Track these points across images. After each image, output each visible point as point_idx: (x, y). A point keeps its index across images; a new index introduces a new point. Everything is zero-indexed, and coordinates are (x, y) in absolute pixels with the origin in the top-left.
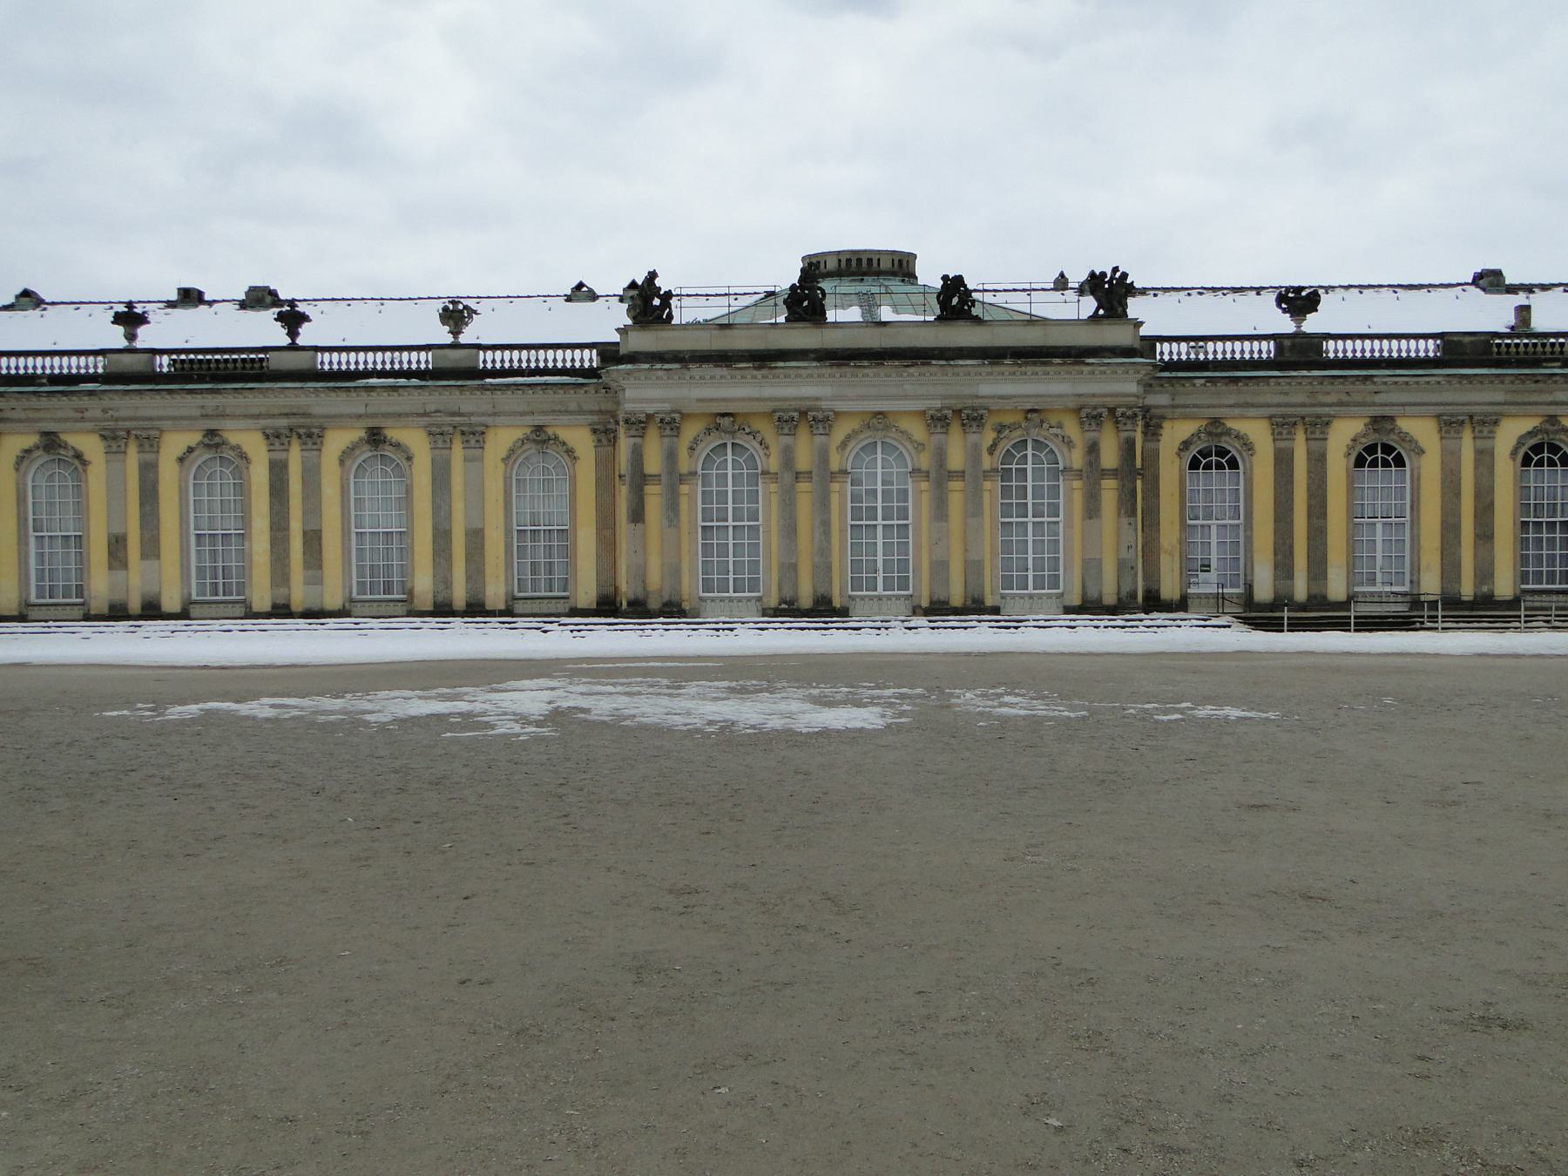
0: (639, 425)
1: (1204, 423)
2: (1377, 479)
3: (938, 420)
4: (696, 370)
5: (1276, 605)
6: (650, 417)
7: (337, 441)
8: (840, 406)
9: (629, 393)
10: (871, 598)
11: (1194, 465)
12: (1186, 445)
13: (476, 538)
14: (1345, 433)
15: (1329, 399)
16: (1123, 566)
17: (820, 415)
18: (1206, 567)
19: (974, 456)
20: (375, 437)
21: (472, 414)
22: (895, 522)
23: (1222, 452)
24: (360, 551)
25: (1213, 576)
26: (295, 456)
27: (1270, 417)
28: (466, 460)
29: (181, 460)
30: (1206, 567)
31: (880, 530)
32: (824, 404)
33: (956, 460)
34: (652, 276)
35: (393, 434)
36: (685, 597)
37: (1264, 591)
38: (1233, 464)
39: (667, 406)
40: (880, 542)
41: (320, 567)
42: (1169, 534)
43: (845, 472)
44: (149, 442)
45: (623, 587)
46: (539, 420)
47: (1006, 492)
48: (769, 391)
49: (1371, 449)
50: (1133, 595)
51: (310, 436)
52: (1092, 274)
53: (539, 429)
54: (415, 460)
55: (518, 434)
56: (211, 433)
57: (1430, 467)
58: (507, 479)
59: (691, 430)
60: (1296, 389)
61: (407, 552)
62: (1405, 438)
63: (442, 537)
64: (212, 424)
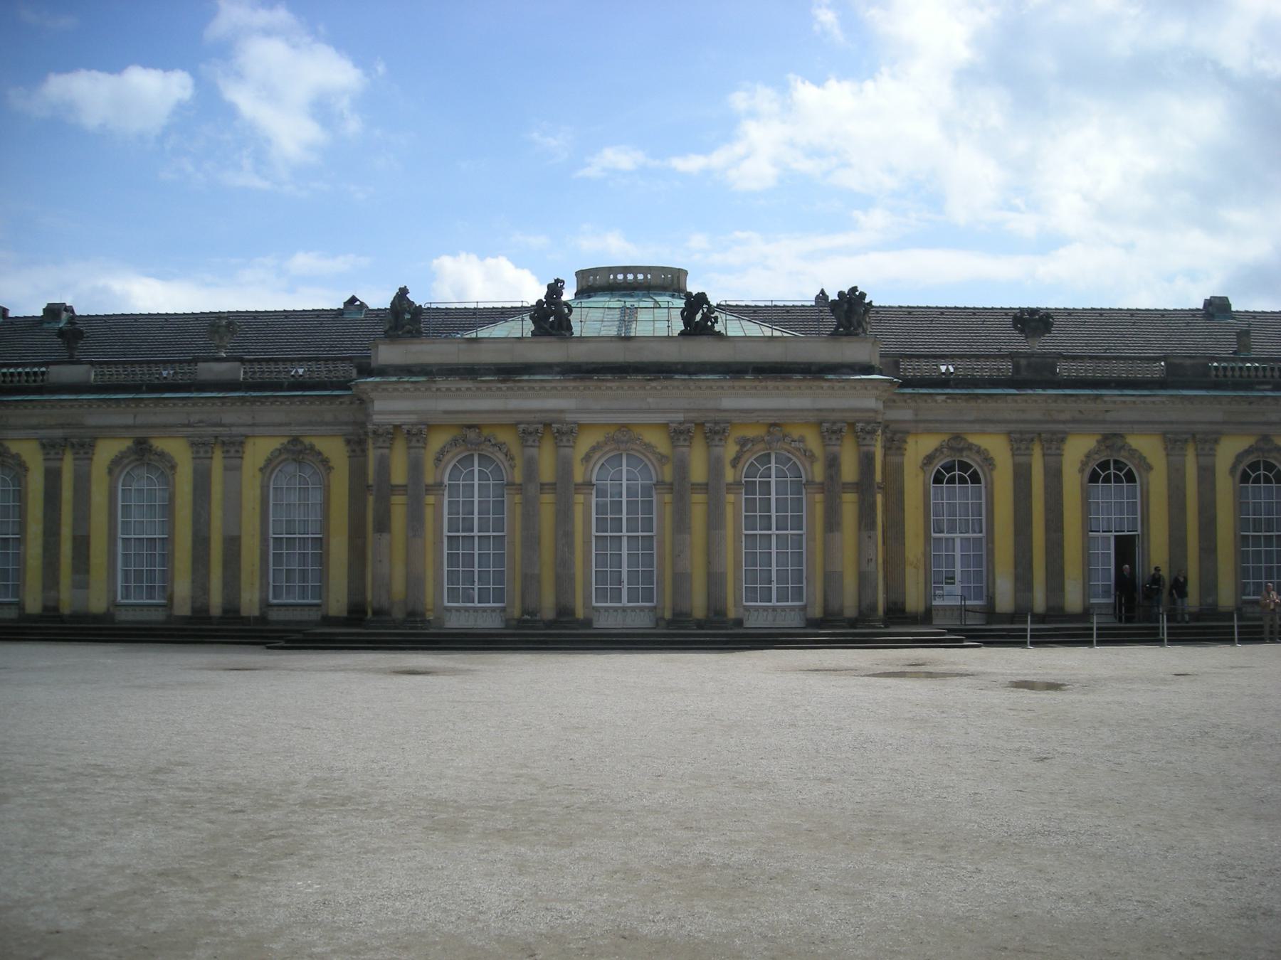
1: (946, 438)
3: (678, 434)
4: (442, 383)
5: (1018, 615)
6: (397, 427)
7: (107, 450)
8: (584, 418)
9: (378, 405)
10: (616, 609)
11: (938, 480)
12: (929, 460)
13: (233, 544)
14: (1077, 449)
15: (1063, 417)
16: (863, 579)
17: (565, 428)
18: (950, 579)
19: (715, 467)
21: (232, 425)
22: (640, 534)
23: (964, 466)
24: (126, 556)
25: (957, 588)
27: (1009, 433)
28: (226, 469)
30: (950, 579)
31: (625, 542)
32: (569, 417)
33: (698, 472)
34: (403, 292)
35: (160, 444)
36: (429, 607)
37: (1005, 600)
38: (975, 479)
39: (413, 418)
40: (625, 552)
41: (87, 571)
42: (914, 547)
43: (589, 484)
45: (369, 596)
46: (296, 431)
47: (750, 504)
48: (513, 404)
49: (1104, 465)
50: (874, 608)
51: (82, 446)
52: (854, 289)
53: (295, 440)
54: (179, 469)
55: (275, 444)
57: (1157, 482)
58: (264, 488)
59: (437, 441)
60: (1033, 405)
61: (168, 559)
62: (1133, 452)
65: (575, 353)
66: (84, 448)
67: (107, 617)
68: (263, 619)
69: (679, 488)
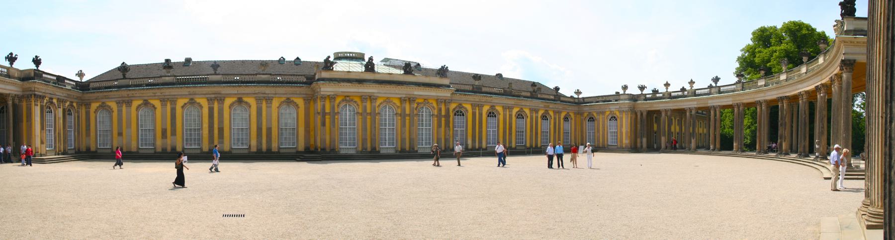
0: (324, 98)
2: (491, 120)
3: (402, 100)
4: (342, 84)
7: (228, 101)
13: (269, 130)
14: (486, 109)
20: (240, 101)
26: (216, 106)
29: (183, 107)
35: (245, 99)
44: (173, 102)
46: (288, 96)
48: (361, 90)
53: (288, 99)
56: (192, 99)
59: (338, 100)
60: (477, 98)
63: (259, 129)
64: (191, 97)
65: (377, 77)
66: (221, 100)
67: (230, 152)
68: (278, 152)
69: (403, 115)
